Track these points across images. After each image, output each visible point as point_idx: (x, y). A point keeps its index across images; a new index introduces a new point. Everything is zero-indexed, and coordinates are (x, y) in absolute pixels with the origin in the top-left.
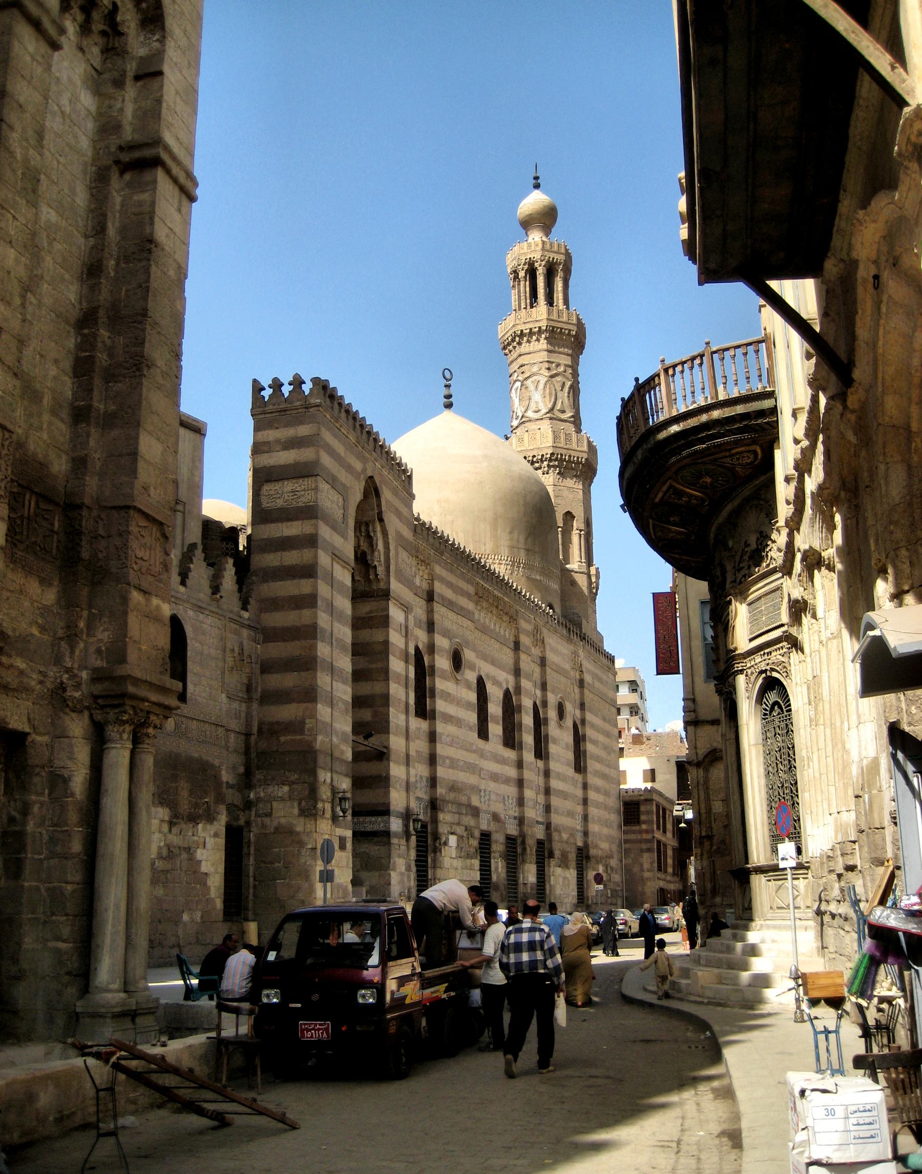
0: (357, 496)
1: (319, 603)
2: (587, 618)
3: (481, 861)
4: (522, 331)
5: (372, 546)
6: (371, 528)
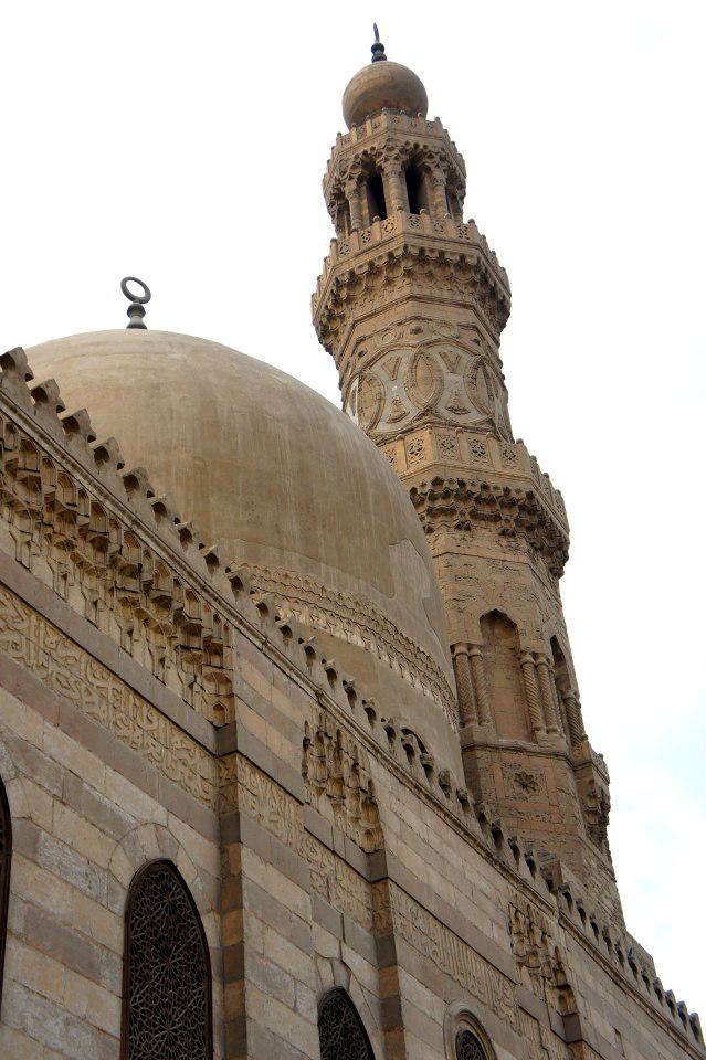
4: (352, 273)
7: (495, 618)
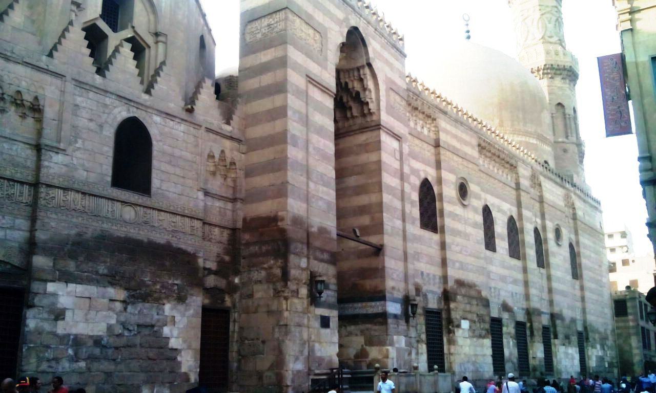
0: (338, 37)
1: (290, 113)
2: (578, 173)
3: (492, 340)
5: (364, 86)
6: (361, 72)
7: (559, 104)
